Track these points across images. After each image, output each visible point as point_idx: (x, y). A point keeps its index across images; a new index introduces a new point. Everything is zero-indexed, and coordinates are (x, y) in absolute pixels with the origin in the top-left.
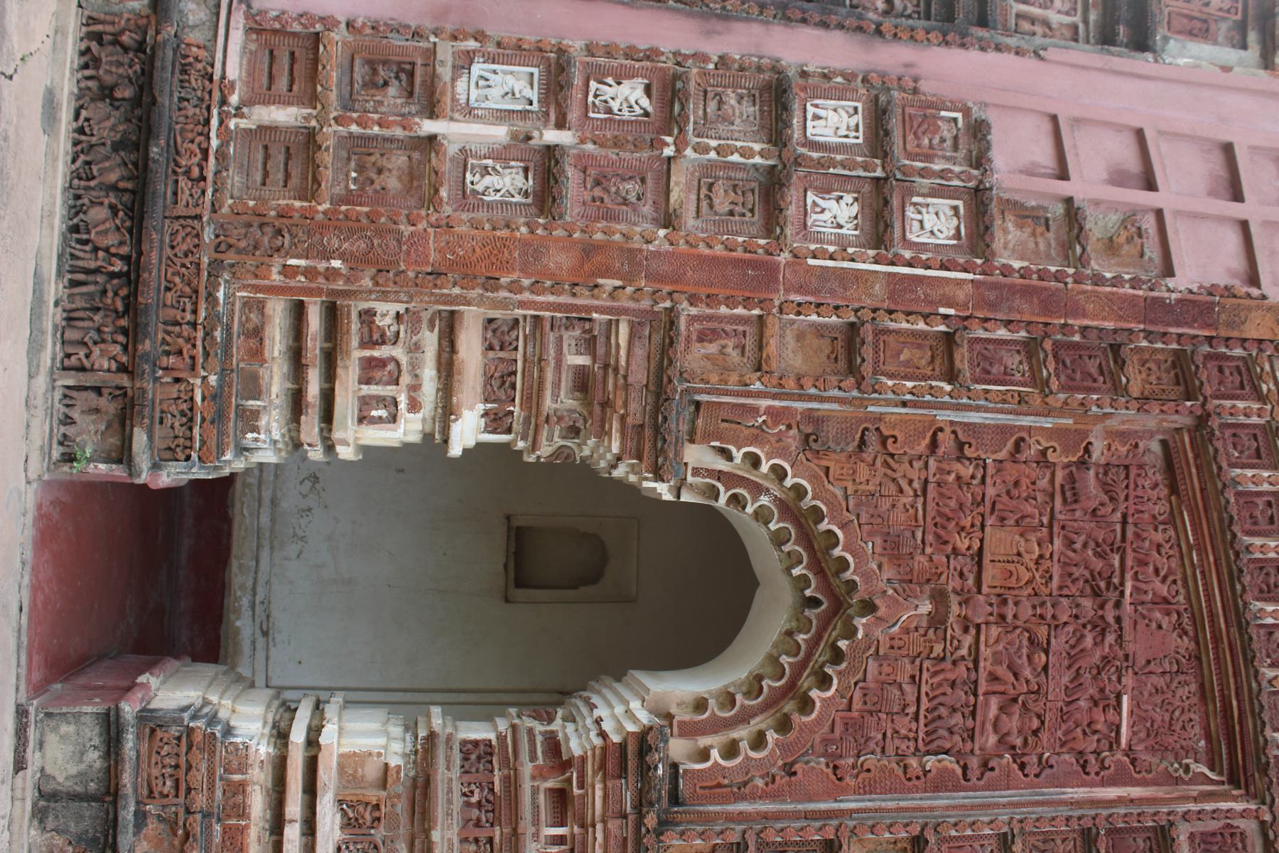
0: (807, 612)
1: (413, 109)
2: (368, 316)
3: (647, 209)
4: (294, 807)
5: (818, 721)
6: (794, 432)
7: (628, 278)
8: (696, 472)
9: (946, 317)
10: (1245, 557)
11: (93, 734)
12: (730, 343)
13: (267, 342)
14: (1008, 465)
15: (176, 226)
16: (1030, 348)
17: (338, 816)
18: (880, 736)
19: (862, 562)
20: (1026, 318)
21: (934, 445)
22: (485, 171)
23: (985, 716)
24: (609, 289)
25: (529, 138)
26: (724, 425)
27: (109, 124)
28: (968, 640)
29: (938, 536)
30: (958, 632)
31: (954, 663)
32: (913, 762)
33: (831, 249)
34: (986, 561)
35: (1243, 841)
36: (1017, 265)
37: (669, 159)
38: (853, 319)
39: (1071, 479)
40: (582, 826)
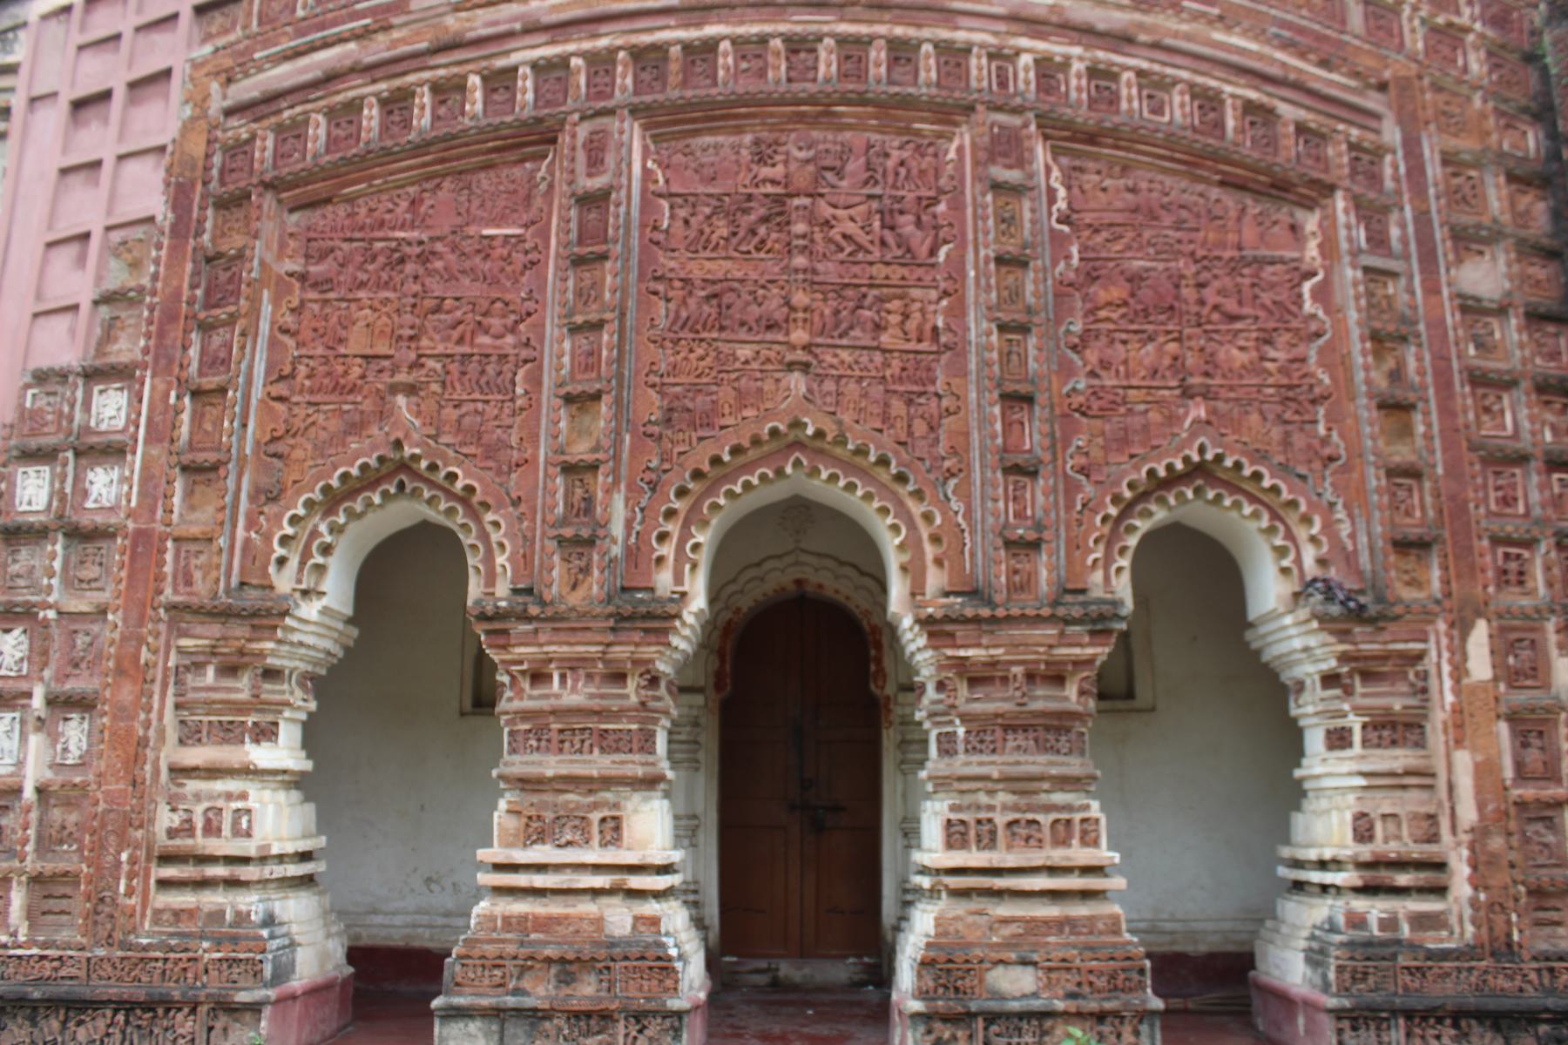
0: (408, 491)
1: (17, 805)
2: (172, 833)
3: (96, 628)
4: (521, 880)
5: (480, 480)
6: (266, 509)
7: (141, 640)
8: (299, 581)
9: (178, 397)
10: (372, 146)
11: (456, 1028)
12: (194, 562)
13: (183, 906)
14: (300, 338)
15: (94, 976)
16: (206, 328)
17: (535, 847)
18: (499, 431)
19: (362, 454)
20: (180, 334)
21: (281, 399)
22: (65, 750)
23: (488, 346)
24: (149, 656)
25: (39, 719)
28: (431, 363)
29: (351, 391)
30: (423, 372)
31: (448, 373)
32: (519, 403)
33: (126, 488)
34: (369, 352)
35: (597, 133)
36: (142, 343)
37: (60, 613)
38: (177, 470)
39: (315, 285)
40: (550, 661)
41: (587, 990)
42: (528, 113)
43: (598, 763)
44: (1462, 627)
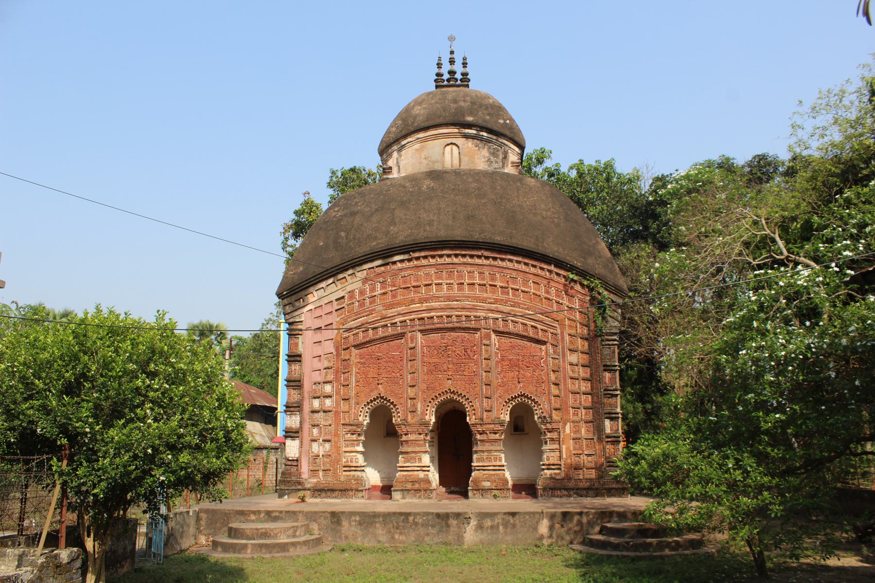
19: (374, 395)
26: (357, 417)
27: (323, 494)
41: (417, 486)
42: (400, 331)
43: (418, 449)
44: (565, 424)
